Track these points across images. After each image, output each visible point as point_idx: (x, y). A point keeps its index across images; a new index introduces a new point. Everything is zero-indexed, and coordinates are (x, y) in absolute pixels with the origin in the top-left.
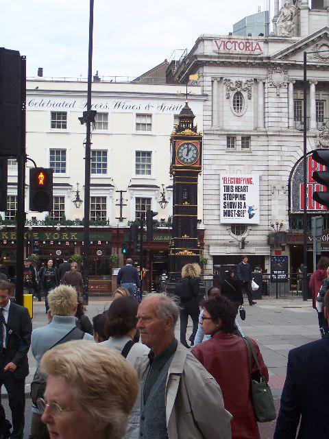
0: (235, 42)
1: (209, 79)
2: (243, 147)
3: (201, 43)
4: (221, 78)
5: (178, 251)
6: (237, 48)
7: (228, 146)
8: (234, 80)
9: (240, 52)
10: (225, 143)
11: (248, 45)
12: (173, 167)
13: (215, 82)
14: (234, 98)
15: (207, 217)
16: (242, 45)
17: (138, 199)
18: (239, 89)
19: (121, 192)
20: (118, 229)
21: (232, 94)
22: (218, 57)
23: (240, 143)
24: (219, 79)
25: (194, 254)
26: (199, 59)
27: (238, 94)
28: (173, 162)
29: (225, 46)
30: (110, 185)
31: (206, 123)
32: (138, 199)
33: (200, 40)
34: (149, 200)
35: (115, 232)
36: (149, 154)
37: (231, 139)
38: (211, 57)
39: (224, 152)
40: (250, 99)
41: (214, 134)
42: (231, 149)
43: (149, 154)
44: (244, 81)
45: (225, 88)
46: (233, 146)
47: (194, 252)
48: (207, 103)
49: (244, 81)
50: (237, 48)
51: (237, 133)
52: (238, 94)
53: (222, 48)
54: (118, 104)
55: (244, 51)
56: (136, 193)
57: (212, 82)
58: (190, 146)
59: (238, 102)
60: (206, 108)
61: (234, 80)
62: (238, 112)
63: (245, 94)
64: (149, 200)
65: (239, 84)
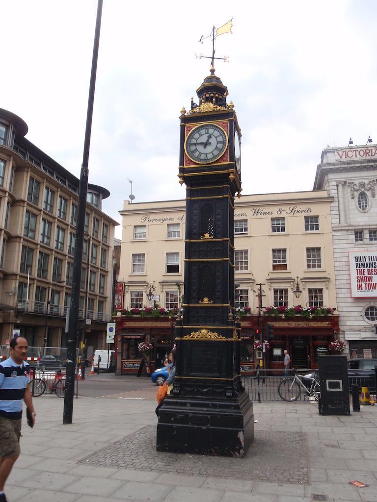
0: (356, 151)
1: (335, 184)
2: (371, 239)
3: (325, 156)
4: (345, 182)
5: (189, 331)
6: (358, 155)
7: (357, 240)
8: (357, 182)
9: (362, 158)
10: (353, 237)
11: (368, 151)
12: (182, 170)
13: (340, 186)
14: (359, 198)
15: (341, 305)
16: (362, 153)
17: (276, 291)
18: (363, 190)
19: (261, 284)
20: (259, 316)
21: (357, 194)
22: (341, 164)
23: (368, 236)
24: (343, 183)
25: (224, 339)
26: (323, 168)
27: (362, 195)
28: (182, 162)
29: (347, 155)
30: (250, 279)
31: (333, 221)
32: (276, 291)
33: (325, 153)
34: (286, 291)
35: (256, 319)
36: (284, 250)
37: (359, 234)
38: (334, 164)
39: (353, 245)
40: (374, 197)
41: (342, 230)
42: (359, 242)
43: (284, 250)
44: (367, 182)
45: (349, 190)
46: (361, 240)
47: (220, 332)
48: (333, 204)
49: (367, 182)
50: (358, 155)
51: (364, 227)
52: (362, 195)
53: (344, 157)
54: (257, 211)
55: (364, 158)
56: (273, 285)
57: (337, 186)
58: (211, 131)
59: (363, 204)
60: (332, 208)
61: (357, 182)
62: (364, 209)
63: (369, 193)
64: (286, 291)
65: (362, 185)
